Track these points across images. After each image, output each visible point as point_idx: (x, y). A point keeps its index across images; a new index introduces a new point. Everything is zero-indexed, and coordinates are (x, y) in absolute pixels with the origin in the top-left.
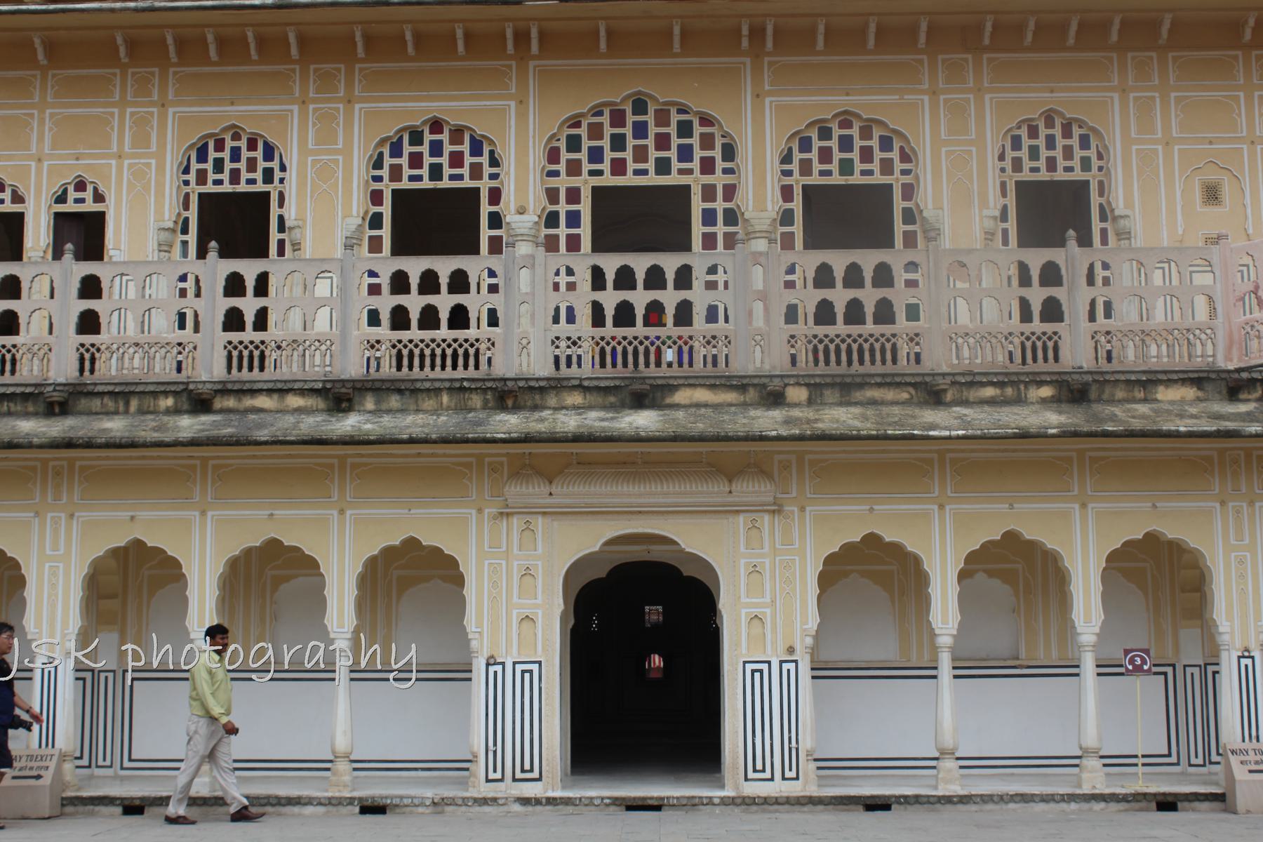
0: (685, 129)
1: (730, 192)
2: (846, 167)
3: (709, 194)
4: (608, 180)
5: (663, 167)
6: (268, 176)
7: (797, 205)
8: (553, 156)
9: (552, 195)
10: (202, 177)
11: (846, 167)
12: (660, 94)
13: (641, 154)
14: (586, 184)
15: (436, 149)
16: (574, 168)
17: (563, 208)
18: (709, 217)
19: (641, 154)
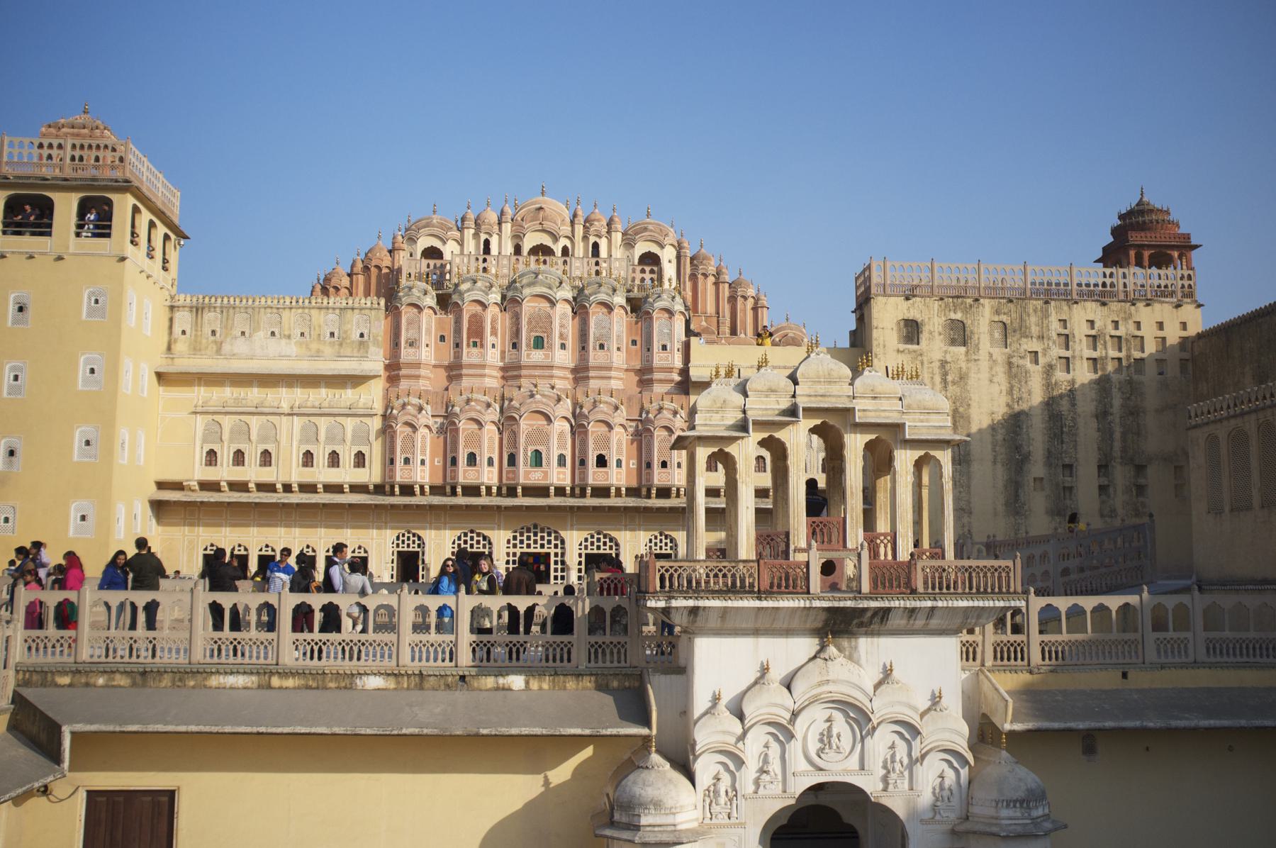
0: (549, 535)
1: (563, 554)
2: (599, 548)
3: (556, 555)
4: (525, 550)
5: (542, 546)
6: (419, 546)
7: (583, 559)
8: (509, 542)
9: (508, 554)
10: (398, 545)
11: (599, 548)
12: (542, 524)
13: (535, 542)
14: (518, 551)
15: (472, 539)
16: (515, 546)
17: (511, 558)
18: (556, 563)
19: (535, 542)
